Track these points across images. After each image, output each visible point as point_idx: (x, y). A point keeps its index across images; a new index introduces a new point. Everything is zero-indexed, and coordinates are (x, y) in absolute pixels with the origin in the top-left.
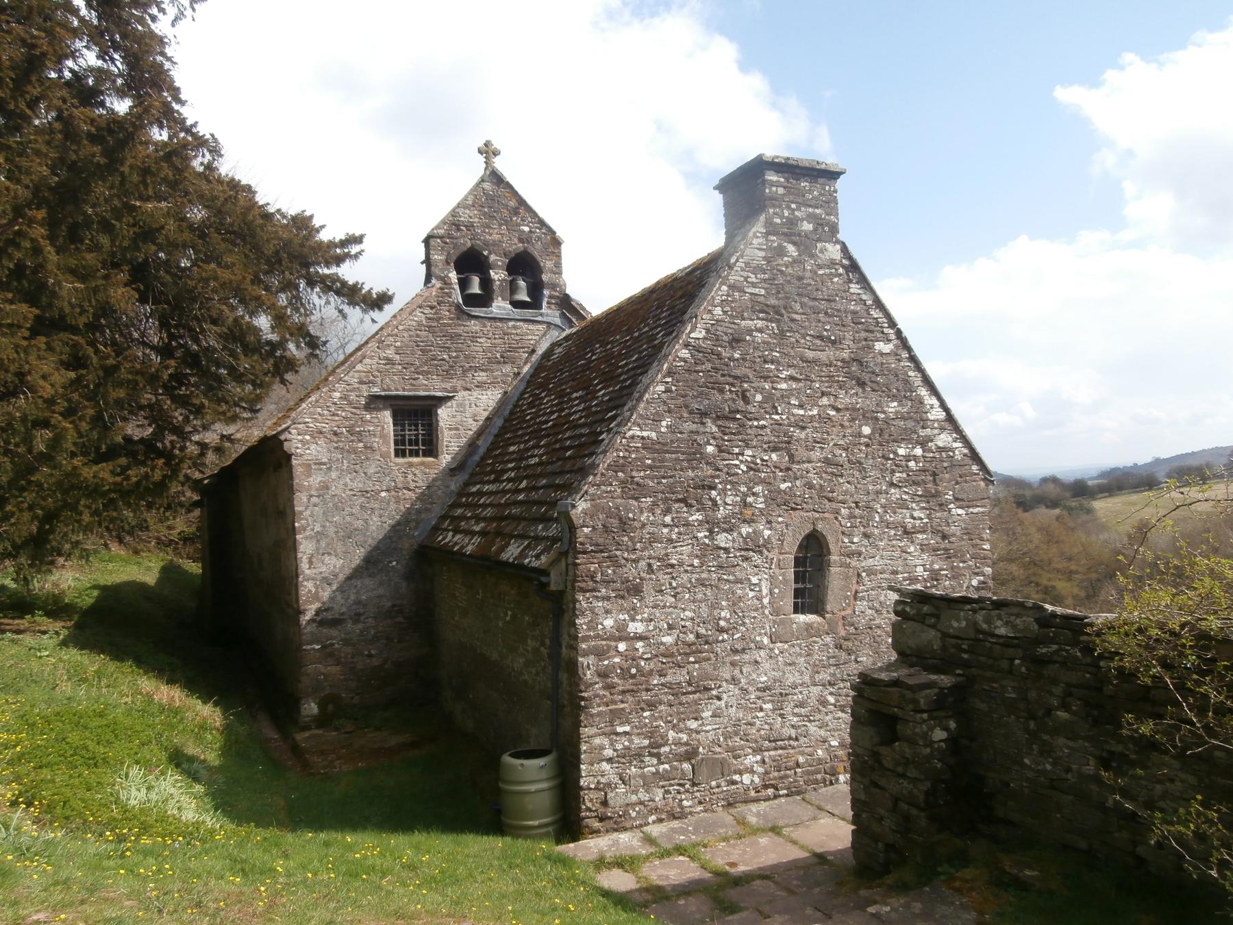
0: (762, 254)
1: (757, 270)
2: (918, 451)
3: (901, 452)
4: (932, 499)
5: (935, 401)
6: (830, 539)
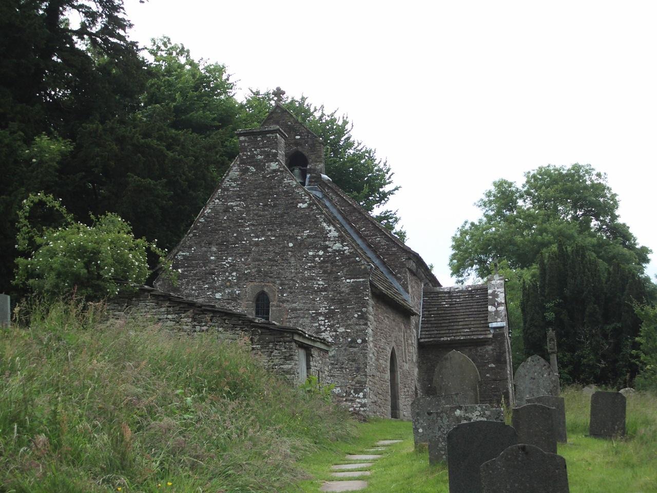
0: (237, 173)
1: (235, 180)
2: (321, 253)
3: (311, 253)
4: (331, 276)
5: (332, 228)
6: (270, 295)
